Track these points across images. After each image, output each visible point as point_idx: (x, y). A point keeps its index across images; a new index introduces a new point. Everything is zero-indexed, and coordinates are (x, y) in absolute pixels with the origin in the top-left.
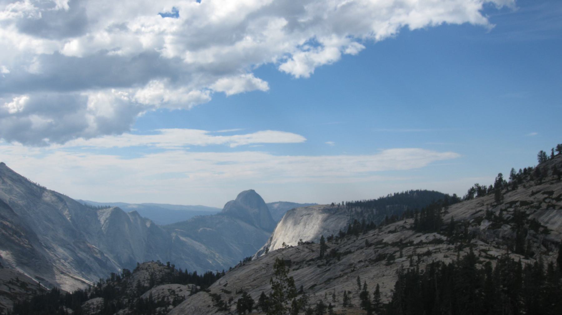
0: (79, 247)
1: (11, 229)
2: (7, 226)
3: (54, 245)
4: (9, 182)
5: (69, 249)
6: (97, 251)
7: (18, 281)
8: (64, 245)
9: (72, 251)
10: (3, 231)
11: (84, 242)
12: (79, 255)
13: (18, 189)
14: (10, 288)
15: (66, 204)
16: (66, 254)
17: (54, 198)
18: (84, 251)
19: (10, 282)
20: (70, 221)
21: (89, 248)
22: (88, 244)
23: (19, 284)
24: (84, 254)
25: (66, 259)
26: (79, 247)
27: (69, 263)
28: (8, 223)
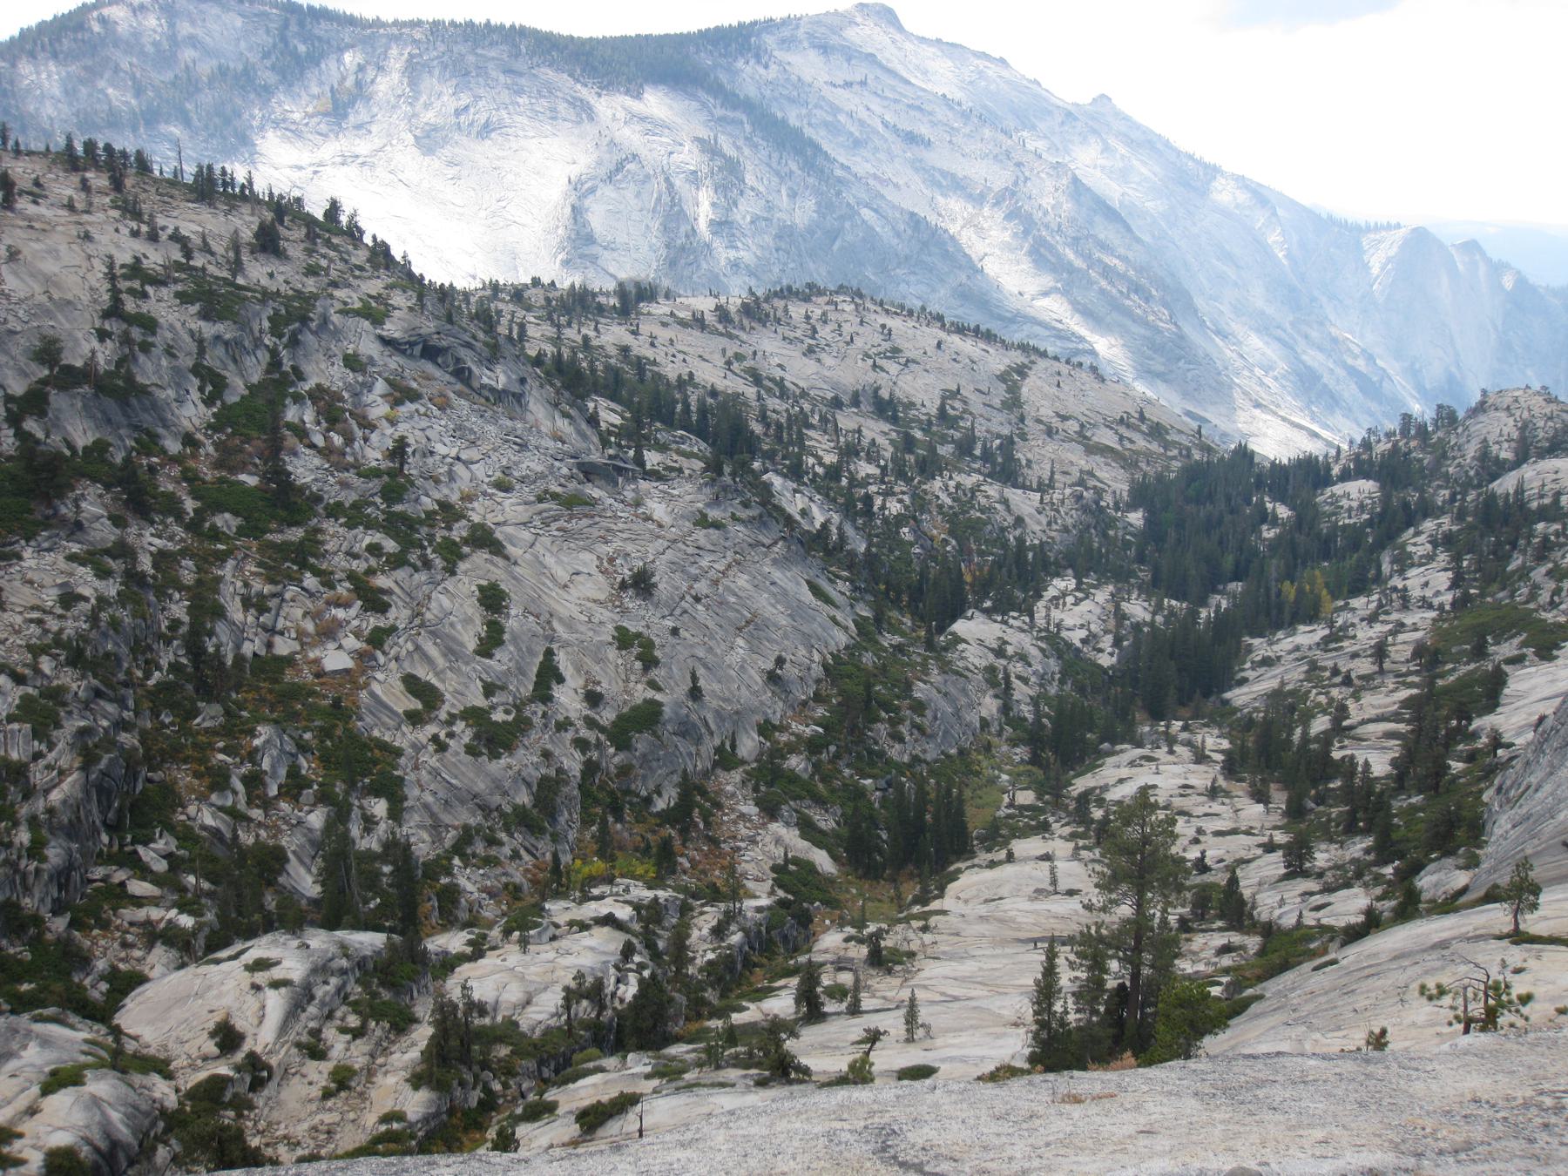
0: (1306, 337)
1: (1123, 277)
3: (1236, 327)
4: (1122, 150)
5: (1279, 340)
6: (1357, 351)
7: (1142, 418)
8: (1265, 328)
10: (1104, 283)
11: (1321, 324)
12: (1304, 357)
13: (1145, 168)
14: (1121, 438)
15: (1274, 214)
16: (1269, 352)
17: (1243, 197)
18: (1320, 349)
20: (1285, 262)
21: (1335, 340)
22: (1333, 330)
23: (1144, 428)
24: (1321, 357)
25: (1267, 369)
26: (1306, 337)
27: (1276, 379)
28: (1116, 261)
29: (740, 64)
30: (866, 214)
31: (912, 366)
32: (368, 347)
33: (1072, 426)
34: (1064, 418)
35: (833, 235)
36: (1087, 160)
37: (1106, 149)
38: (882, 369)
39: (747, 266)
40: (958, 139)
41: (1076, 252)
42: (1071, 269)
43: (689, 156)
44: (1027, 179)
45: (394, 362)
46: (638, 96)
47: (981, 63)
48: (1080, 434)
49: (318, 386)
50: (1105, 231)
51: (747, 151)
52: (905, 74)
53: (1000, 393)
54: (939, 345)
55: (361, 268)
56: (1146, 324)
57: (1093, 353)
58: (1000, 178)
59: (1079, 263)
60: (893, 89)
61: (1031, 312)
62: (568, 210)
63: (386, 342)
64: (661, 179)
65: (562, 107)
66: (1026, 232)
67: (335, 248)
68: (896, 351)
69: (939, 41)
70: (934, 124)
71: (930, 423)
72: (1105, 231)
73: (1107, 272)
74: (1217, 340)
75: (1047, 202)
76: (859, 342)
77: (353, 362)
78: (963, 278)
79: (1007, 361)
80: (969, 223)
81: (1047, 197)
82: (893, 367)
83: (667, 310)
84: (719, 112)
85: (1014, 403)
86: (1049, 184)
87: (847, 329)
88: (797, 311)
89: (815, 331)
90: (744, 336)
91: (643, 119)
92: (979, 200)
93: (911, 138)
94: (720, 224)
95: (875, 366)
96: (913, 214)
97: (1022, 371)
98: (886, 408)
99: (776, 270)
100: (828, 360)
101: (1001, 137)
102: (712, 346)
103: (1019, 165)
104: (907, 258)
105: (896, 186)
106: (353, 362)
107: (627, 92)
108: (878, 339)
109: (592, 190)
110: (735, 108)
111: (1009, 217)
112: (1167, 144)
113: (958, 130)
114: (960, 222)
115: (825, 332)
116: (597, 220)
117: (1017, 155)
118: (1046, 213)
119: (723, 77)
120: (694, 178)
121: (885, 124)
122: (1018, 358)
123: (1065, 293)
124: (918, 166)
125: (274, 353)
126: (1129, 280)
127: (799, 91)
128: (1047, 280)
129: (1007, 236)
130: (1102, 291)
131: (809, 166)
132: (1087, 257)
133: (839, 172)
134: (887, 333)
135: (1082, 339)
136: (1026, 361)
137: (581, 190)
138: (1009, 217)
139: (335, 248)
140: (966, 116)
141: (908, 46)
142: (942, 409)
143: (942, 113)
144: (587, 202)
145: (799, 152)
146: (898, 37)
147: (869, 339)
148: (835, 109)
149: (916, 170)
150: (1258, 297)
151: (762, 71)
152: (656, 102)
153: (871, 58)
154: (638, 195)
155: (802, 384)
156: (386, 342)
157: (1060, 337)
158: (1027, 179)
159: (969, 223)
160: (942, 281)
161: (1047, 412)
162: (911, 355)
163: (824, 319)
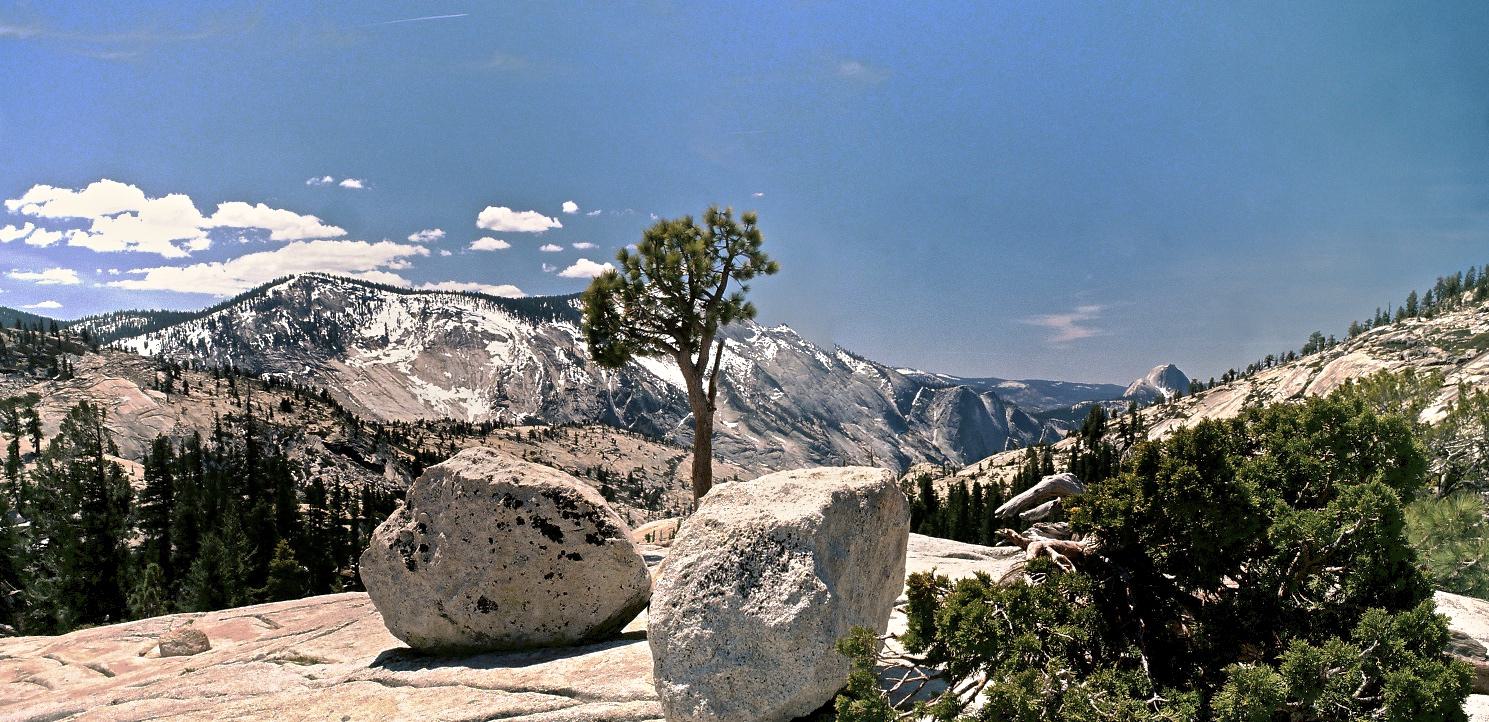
32: (319, 447)
45: (327, 452)
49: (293, 460)
53: (666, 468)
55: (326, 417)
63: (327, 446)
67: (317, 408)
71: (622, 482)
76: (599, 447)
77: (309, 452)
79: (674, 455)
82: (613, 458)
83: (505, 432)
87: (595, 440)
88: (571, 432)
89: (577, 442)
97: (680, 459)
100: (580, 455)
106: (309, 452)
115: (582, 442)
122: (680, 452)
125: (277, 447)
134: (614, 442)
136: (684, 454)
139: (317, 408)
142: (630, 475)
147: (606, 444)
156: (327, 446)
162: (622, 452)
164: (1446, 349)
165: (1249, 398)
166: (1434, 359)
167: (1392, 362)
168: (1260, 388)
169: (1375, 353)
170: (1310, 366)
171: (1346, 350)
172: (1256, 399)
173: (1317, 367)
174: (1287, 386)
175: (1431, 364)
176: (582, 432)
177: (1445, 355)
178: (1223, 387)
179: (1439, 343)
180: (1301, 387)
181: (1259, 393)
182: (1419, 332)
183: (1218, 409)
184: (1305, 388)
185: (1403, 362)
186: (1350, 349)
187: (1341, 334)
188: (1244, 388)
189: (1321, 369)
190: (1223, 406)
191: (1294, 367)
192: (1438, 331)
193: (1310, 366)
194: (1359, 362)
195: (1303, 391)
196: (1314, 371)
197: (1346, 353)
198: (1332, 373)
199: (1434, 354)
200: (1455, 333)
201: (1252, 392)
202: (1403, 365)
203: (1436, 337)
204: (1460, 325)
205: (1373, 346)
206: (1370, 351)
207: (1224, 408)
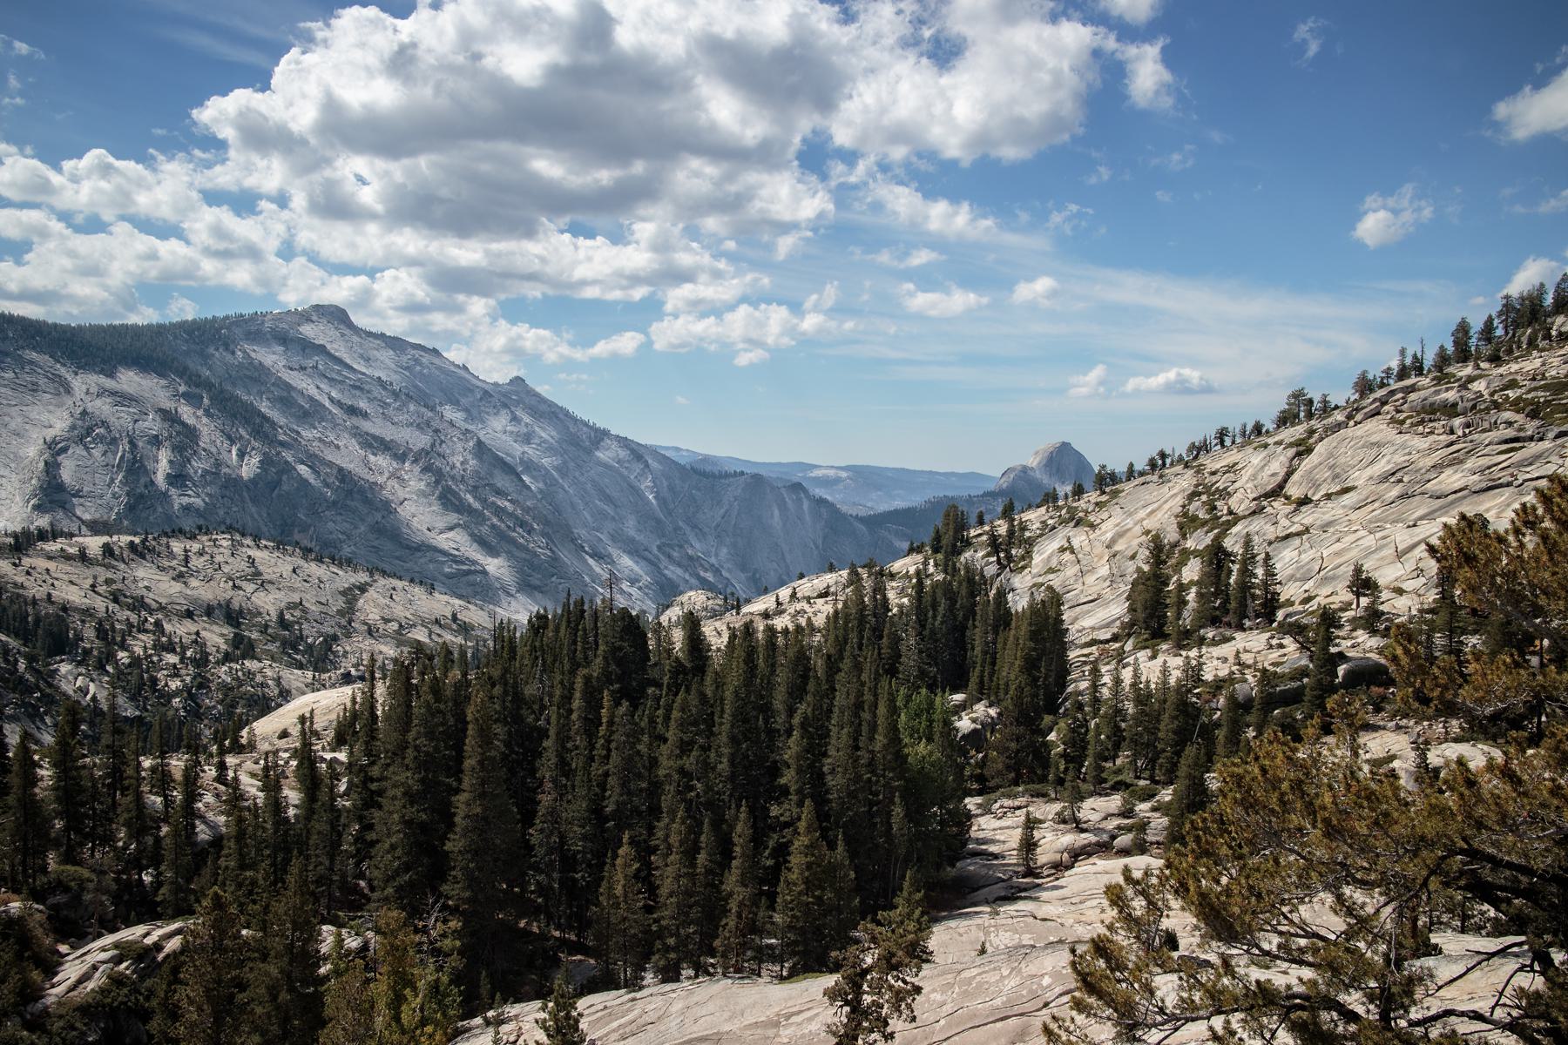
0: (669, 557)
1: (511, 515)
2: (504, 510)
3: (614, 552)
4: (527, 419)
5: (645, 559)
7: (455, 618)
8: (635, 551)
9: (653, 564)
10: (495, 520)
11: (681, 547)
13: (546, 433)
14: (430, 633)
15: (647, 465)
16: (636, 568)
17: (623, 453)
18: (679, 565)
19: (437, 622)
24: (679, 571)
25: (633, 582)
26: (669, 557)
27: (640, 589)
29: (211, 350)
30: (303, 469)
31: (267, 586)
33: (395, 626)
34: (386, 621)
35: (276, 484)
36: (497, 430)
37: (515, 419)
38: (240, 588)
39: (197, 510)
40: (390, 412)
41: (475, 497)
42: (470, 511)
43: (152, 424)
44: (442, 442)
46: (111, 375)
47: (417, 353)
48: (398, 632)
50: (501, 481)
51: (205, 420)
52: (348, 361)
54: (294, 571)
56: (526, 549)
57: (484, 572)
58: (421, 441)
59: (477, 505)
60: (339, 372)
61: (434, 542)
62: (41, 465)
64: (125, 441)
65: (42, 381)
66: (437, 482)
68: (258, 574)
69: (383, 335)
70: (370, 400)
71: (267, 626)
72: (501, 481)
73: (499, 512)
74: (591, 561)
75: (457, 460)
78: (378, 517)
79: (352, 580)
80: (392, 476)
81: (459, 457)
83: (59, 546)
84: (182, 389)
85: (349, 610)
86: (459, 446)
87: (218, 559)
88: (177, 546)
90: (122, 566)
91: (113, 393)
92: (401, 458)
93: (353, 411)
94: (176, 477)
95: (235, 587)
96: (341, 470)
97: (363, 588)
98: (233, 616)
99: (221, 512)
101: (423, 410)
102: (85, 576)
103: (437, 431)
104: (334, 503)
105: (338, 447)
107: (102, 372)
108: (244, 565)
109: (65, 450)
110: (197, 386)
111: (425, 470)
112: (567, 414)
113: (389, 405)
114: (387, 474)
115: (197, 562)
116: (67, 474)
117: (436, 424)
118: (453, 467)
119: (194, 364)
120: (156, 441)
121: (331, 399)
122: (363, 577)
123: (465, 527)
124: (357, 433)
126: (517, 518)
127: (258, 376)
128: (453, 518)
129: (422, 485)
130: (493, 526)
131: (257, 433)
132: (484, 501)
133: (282, 438)
134: (252, 561)
135: (474, 562)
136: (368, 579)
137: (55, 449)
138: (425, 470)
140: (396, 395)
141: (355, 338)
142: (281, 615)
143: (377, 392)
144: (60, 459)
145: (247, 421)
146: (347, 332)
147: (238, 565)
148: (289, 387)
149: (355, 436)
150: (630, 527)
151: (228, 357)
152: (129, 380)
153: (321, 349)
154: (104, 454)
155: (163, 601)
157: (456, 562)
158: (442, 442)
159: (392, 476)
160: (363, 520)
161: (374, 616)
162: (266, 577)
163: (201, 553)
164: (1533, 415)
165: (1194, 495)
166: (1510, 433)
167: (1432, 438)
168: (1209, 480)
169: (1402, 422)
170: (1291, 445)
171: (1350, 417)
172: (1204, 498)
173: (1303, 449)
174: (1254, 477)
175: (1506, 442)
176: (196, 547)
177: (1531, 427)
178: (1149, 478)
179: (1517, 405)
180: (1279, 478)
181: (1208, 490)
182: (1479, 386)
183: (1142, 514)
184: (1285, 481)
185: (1453, 437)
186: (1359, 417)
187: (1342, 394)
188: (1185, 481)
189: (1309, 451)
190: (1149, 509)
191: (1266, 446)
192: (1513, 384)
193: (1291, 445)
194: (1374, 439)
195: (1281, 486)
196: (1299, 454)
197: (1352, 423)
198: (1331, 455)
199: (1510, 424)
200: (1544, 388)
201: (1197, 486)
202: (1452, 444)
203: (1511, 394)
204: (1553, 373)
205: (1398, 411)
206: (1393, 421)
207: (1153, 512)
